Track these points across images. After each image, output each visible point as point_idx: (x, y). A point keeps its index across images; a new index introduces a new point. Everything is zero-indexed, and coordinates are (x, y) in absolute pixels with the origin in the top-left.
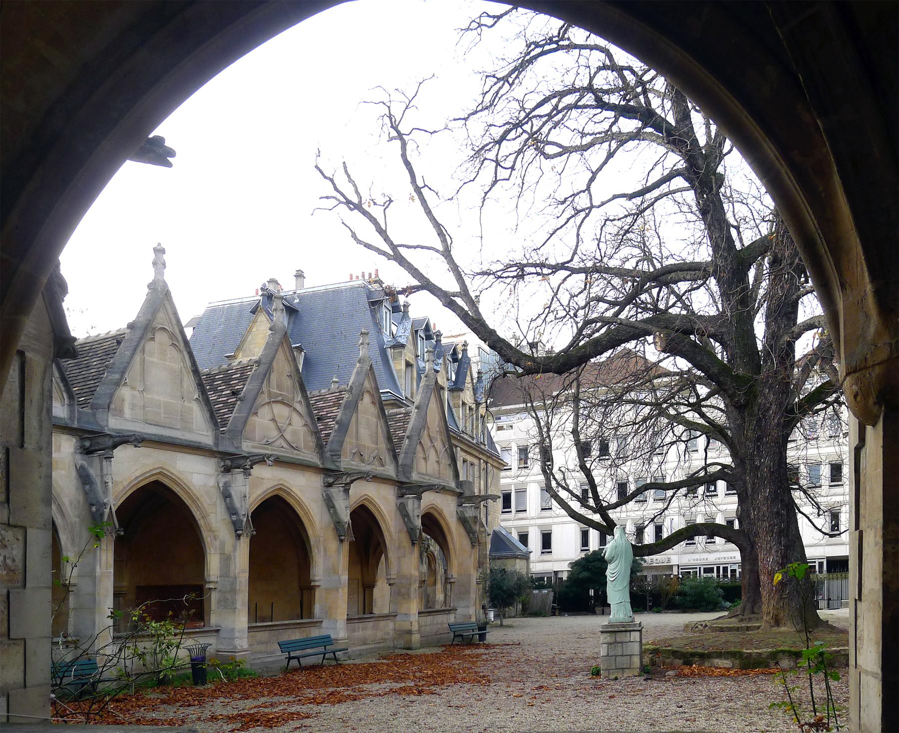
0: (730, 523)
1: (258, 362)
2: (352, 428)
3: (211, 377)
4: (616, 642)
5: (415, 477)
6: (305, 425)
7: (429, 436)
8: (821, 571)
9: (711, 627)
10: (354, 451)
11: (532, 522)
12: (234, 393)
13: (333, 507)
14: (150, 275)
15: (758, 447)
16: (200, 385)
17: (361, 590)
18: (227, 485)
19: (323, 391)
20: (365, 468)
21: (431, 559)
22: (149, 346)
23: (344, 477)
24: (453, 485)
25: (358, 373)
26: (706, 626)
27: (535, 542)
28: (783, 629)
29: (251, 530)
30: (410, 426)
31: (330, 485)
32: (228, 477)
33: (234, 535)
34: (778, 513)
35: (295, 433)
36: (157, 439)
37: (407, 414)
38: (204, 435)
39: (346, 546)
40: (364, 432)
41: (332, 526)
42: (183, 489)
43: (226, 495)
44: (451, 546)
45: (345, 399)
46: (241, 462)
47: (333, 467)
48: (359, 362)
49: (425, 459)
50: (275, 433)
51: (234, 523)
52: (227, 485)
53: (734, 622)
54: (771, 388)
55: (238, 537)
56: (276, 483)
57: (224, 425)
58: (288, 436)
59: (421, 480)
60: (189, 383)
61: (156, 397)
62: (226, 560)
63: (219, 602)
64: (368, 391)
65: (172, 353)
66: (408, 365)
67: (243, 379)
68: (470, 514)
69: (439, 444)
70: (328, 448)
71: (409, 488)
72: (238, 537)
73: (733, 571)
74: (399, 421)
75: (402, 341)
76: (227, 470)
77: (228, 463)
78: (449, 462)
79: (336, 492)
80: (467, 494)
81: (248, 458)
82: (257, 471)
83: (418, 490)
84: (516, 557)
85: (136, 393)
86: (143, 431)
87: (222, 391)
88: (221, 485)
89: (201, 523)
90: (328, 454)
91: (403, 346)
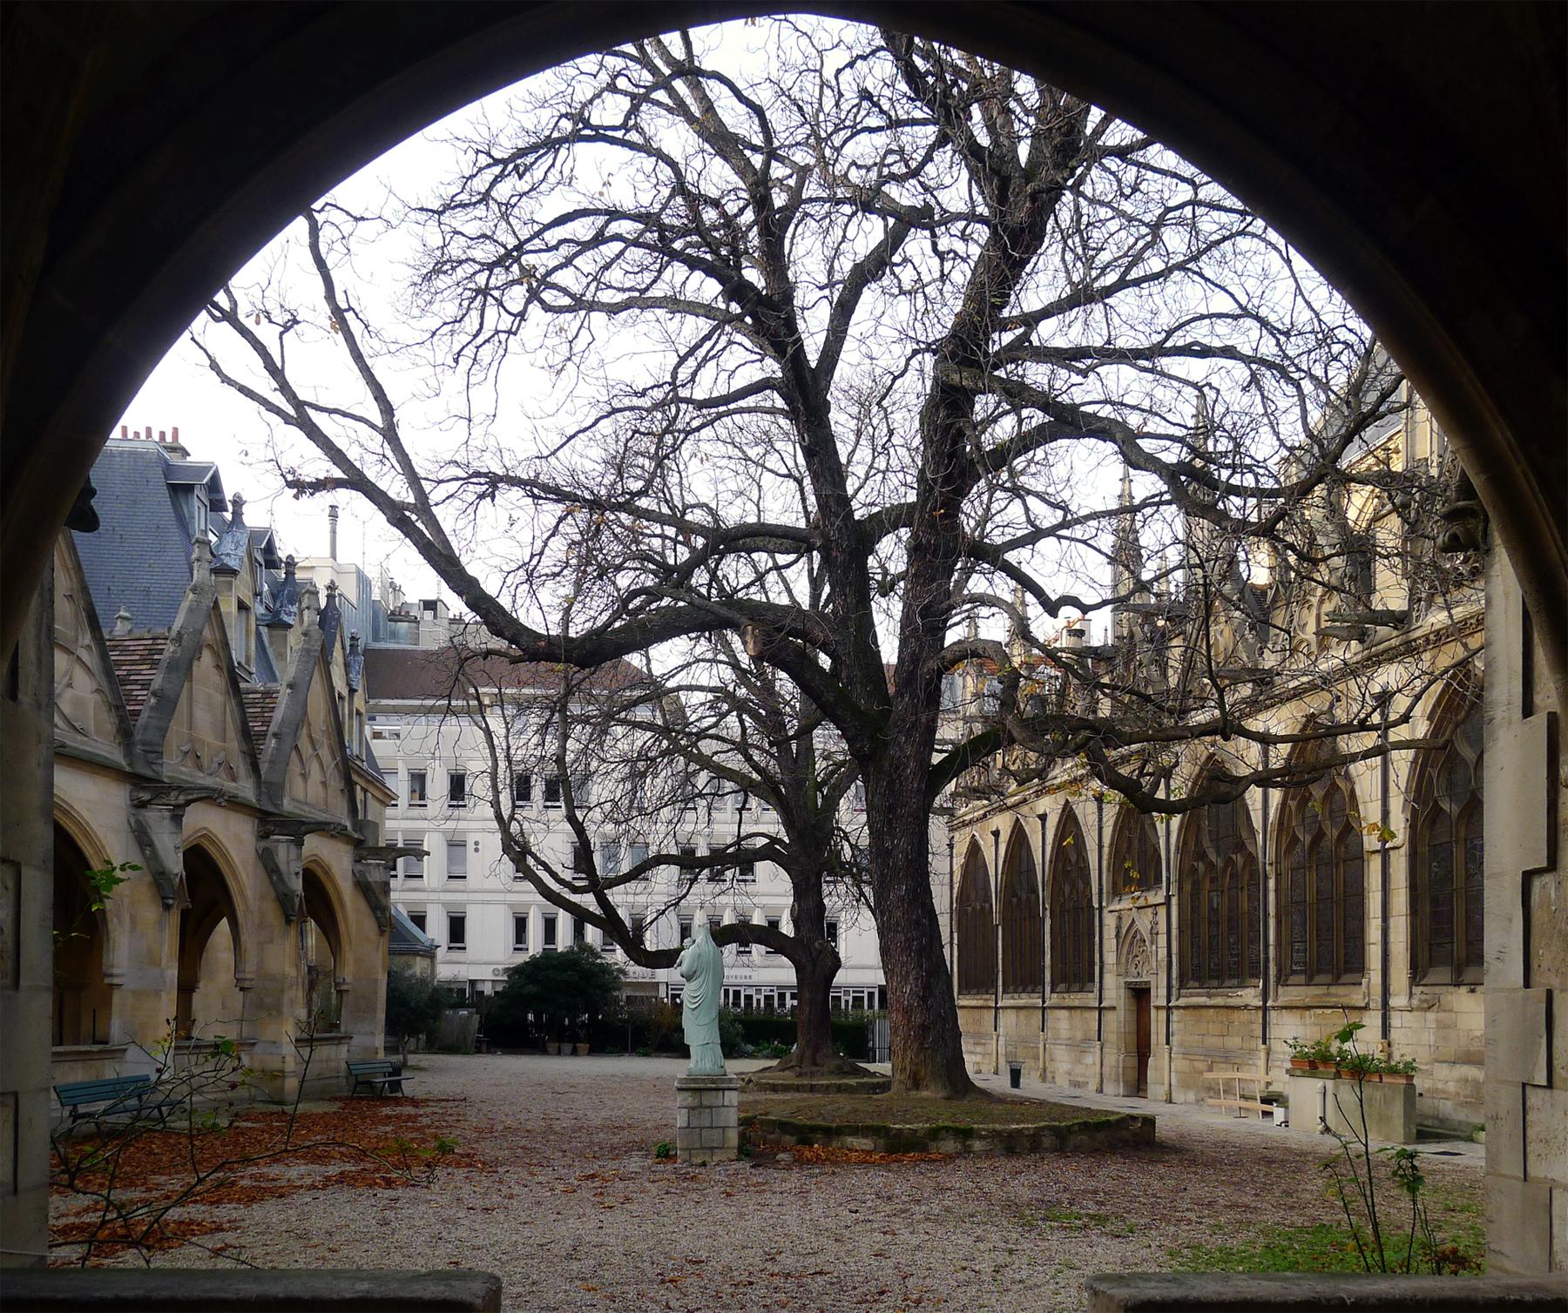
0: (774, 925)
4: (701, 1106)
5: (287, 806)
6: (98, 691)
7: (310, 737)
8: (871, 1006)
9: (757, 1084)
11: (433, 896)
15: (890, 822)
26: (750, 1081)
27: (437, 930)
28: (925, 1094)
31: (142, 805)
34: (917, 922)
39: (175, 918)
40: (203, 718)
47: (148, 772)
53: (788, 1077)
54: (908, 736)
66: (242, 606)
68: (375, 876)
69: (325, 753)
73: (749, 998)
75: (232, 563)
78: (342, 785)
80: (371, 844)
83: (297, 829)
84: (416, 953)
90: (138, 749)
91: (234, 573)
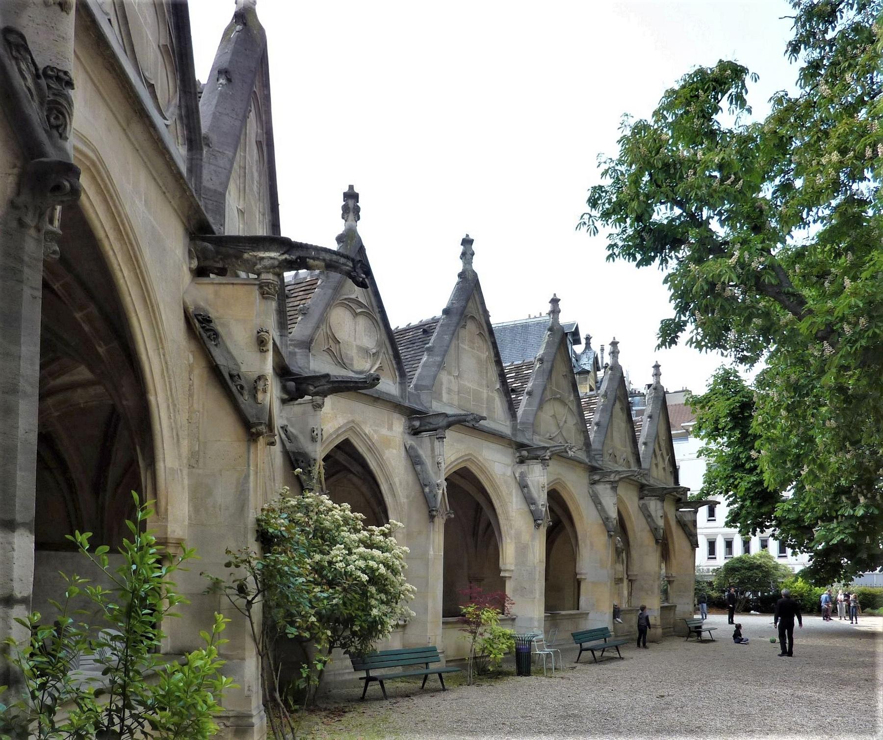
13: (600, 503)
14: (459, 266)
18: (522, 475)
31: (594, 483)
32: (523, 468)
42: (487, 477)
43: (523, 486)
52: (522, 475)
62: (522, 550)
63: (515, 590)
65: (479, 342)
76: (522, 461)
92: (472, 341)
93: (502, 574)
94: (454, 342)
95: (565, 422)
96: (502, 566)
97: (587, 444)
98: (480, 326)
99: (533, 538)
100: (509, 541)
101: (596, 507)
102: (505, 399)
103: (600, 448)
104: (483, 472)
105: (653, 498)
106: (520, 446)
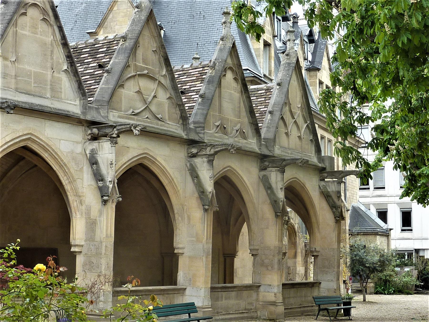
1: (124, 38)
2: (216, 101)
3: (78, 50)
5: (277, 151)
6: (169, 98)
10: (217, 124)
12: (101, 66)
13: (197, 177)
16: (69, 57)
17: (222, 259)
18: (93, 153)
19: (185, 66)
20: (229, 140)
21: (292, 232)
22: (22, 20)
23: (209, 149)
24: (314, 160)
25: (221, 50)
29: (117, 197)
30: (272, 101)
31: (194, 156)
32: (95, 145)
33: (100, 200)
35: (160, 105)
36: (27, 106)
37: (268, 90)
38: (73, 105)
41: (196, 195)
42: (51, 155)
44: (313, 219)
45: (208, 75)
46: (108, 131)
47: (197, 138)
48: (222, 39)
49: (287, 134)
50: (140, 107)
51: (100, 189)
52: (93, 153)
55: (105, 202)
56: (142, 152)
57: (92, 96)
58: (153, 108)
59: (283, 154)
60: (60, 54)
61: (27, 67)
62: (92, 225)
63: (84, 265)
64: (230, 68)
65: (42, 26)
67: (109, 53)
69: (300, 121)
70: (191, 120)
71: (273, 162)
72: (105, 202)
74: (261, 96)
76: (95, 138)
77: (95, 131)
79: (201, 163)
81: (115, 127)
82: (122, 140)
85: (8, 63)
86: (16, 99)
87: (89, 63)
88: (88, 152)
89: (67, 187)
90: (192, 126)
92: (34, 27)
93: (73, 249)
94: (11, 31)
95: (155, 97)
96: (72, 242)
97: (184, 118)
98: (44, 11)
99: (101, 213)
100: (78, 216)
101: (193, 180)
102: (74, 79)
103: (202, 120)
104: (46, 150)
105: (274, 169)
106: (92, 124)
